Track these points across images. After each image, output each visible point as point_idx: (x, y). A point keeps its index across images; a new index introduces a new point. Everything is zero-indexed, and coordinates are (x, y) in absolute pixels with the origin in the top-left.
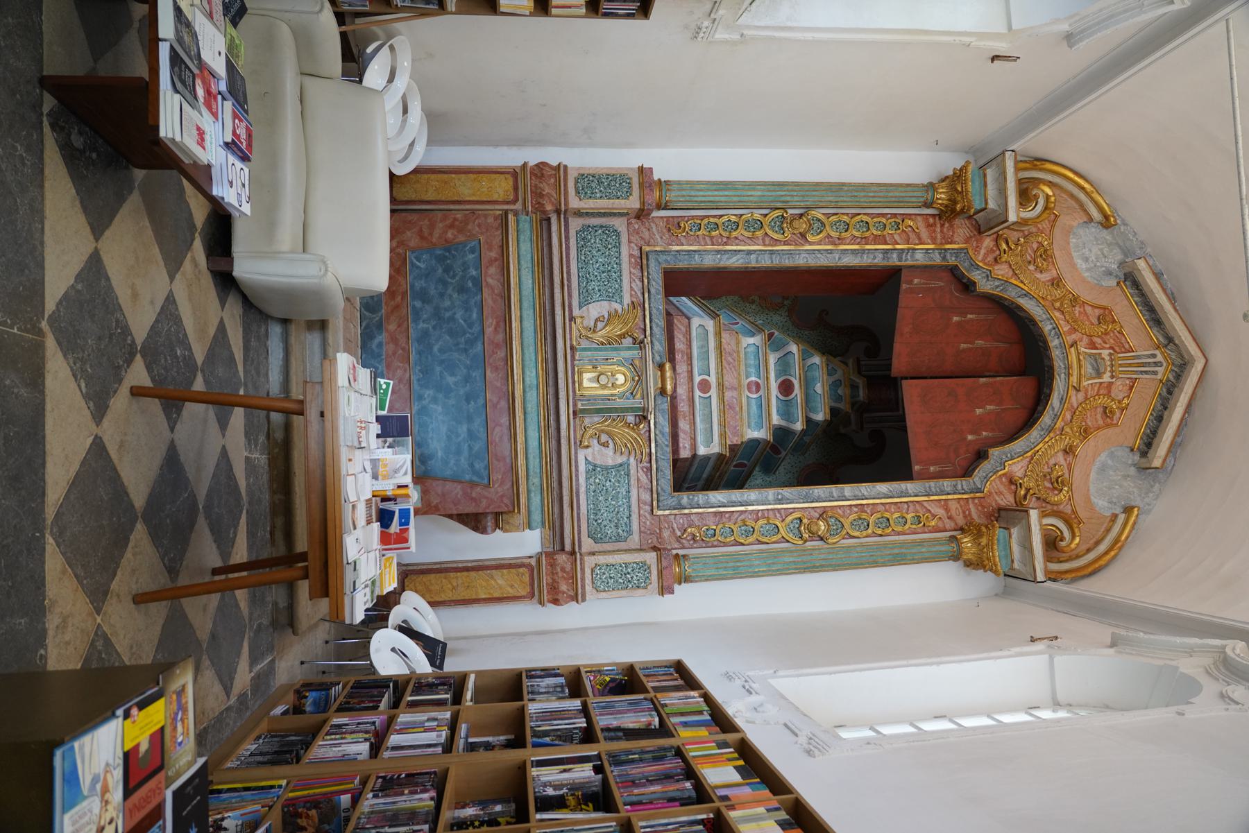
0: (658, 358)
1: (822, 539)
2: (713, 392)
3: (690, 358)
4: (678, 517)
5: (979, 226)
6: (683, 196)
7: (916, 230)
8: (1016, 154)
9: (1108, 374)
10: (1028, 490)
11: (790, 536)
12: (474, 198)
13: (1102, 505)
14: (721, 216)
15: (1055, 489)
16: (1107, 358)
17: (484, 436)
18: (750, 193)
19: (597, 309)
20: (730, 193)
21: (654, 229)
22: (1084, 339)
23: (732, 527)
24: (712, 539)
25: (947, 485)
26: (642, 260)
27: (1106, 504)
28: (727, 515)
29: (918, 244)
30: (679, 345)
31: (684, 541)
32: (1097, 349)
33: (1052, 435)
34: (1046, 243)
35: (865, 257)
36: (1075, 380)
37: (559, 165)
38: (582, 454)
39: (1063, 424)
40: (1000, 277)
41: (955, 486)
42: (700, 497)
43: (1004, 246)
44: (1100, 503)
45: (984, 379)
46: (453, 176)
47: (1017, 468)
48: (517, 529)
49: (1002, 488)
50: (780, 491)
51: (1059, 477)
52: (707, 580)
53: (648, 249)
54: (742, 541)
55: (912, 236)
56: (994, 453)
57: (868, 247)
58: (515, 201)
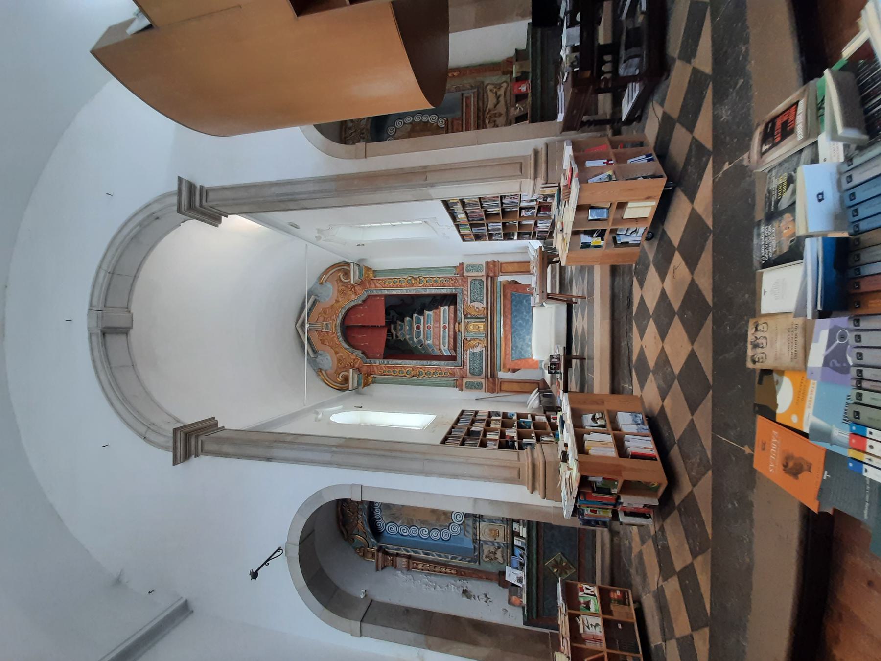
0: (460, 334)
2: (442, 325)
3: (449, 336)
10: (351, 290)
13: (329, 285)
17: (513, 306)
19: (477, 350)
21: (459, 374)
26: (463, 364)
30: (452, 341)
38: (484, 305)
43: (352, 364)
47: (353, 297)
49: (359, 291)
53: (461, 367)
55: (379, 368)
56: (360, 302)
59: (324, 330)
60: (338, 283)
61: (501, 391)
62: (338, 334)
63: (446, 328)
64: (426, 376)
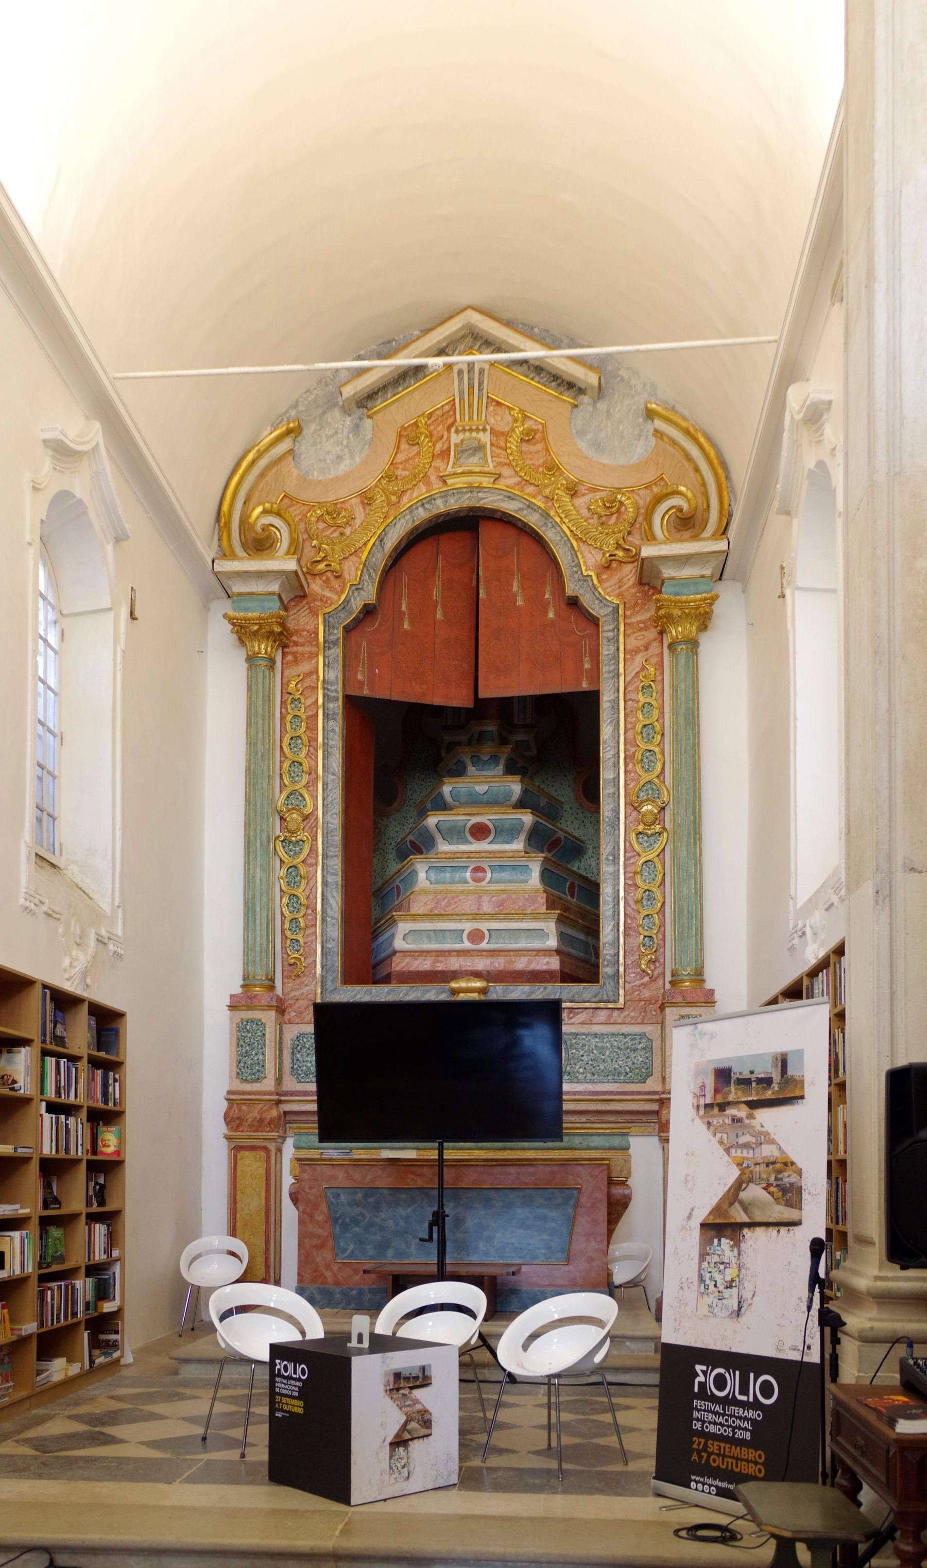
1: (663, 809)
4: (628, 979)
5: (296, 597)
6: (261, 960)
7: (301, 677)
8: (216, 558)
9: (481, 435)
10: (618, 547)
11: (658, 847)
12: (263, 1194)
13: (642, 448)
14: (282, 914)
15: (618, 511)
16: (461, 436)
18: (258, 881)
20: (258, 904)
22: (437, 465)
23: (642, 916)
24: (655, 940)
25: (609, 650)
27: (641, 443)
28: (629, 921)
29: (318, 677)
31: (656, 973)
32: (449, 448)
33: (552, 513)
34: (318, 512)
35: (333, 742)
36: (487, 479)
37: (227, 1100)
39: (540, 497)
40: (359, 573)
41: (609, 640)
42: (606, 952)
43: (321, 566)
44: (639, 450)
45: (481, 591)
46: (238, 1216)
47: (590, 559)
48: (627, 1161)
49: (614, 580)
50: (603, 857)
51: (605, 505)
52: (702, 950)
54: (659, 905)
55: (307, 683)
57: (320, 739)
58: (266, 1149)
59: (455, 439)
60: (648, 487)
61: (236, 1150)
62: (439, 502)
63: (473, 942)
64: (284, 870)
